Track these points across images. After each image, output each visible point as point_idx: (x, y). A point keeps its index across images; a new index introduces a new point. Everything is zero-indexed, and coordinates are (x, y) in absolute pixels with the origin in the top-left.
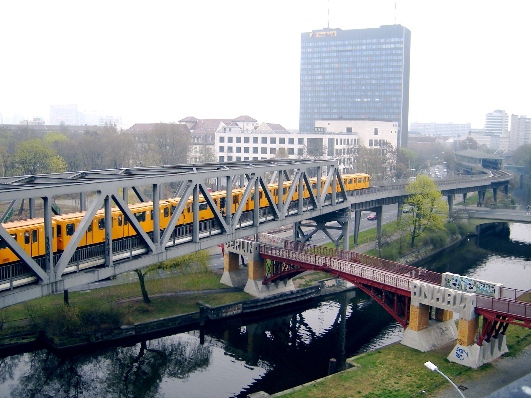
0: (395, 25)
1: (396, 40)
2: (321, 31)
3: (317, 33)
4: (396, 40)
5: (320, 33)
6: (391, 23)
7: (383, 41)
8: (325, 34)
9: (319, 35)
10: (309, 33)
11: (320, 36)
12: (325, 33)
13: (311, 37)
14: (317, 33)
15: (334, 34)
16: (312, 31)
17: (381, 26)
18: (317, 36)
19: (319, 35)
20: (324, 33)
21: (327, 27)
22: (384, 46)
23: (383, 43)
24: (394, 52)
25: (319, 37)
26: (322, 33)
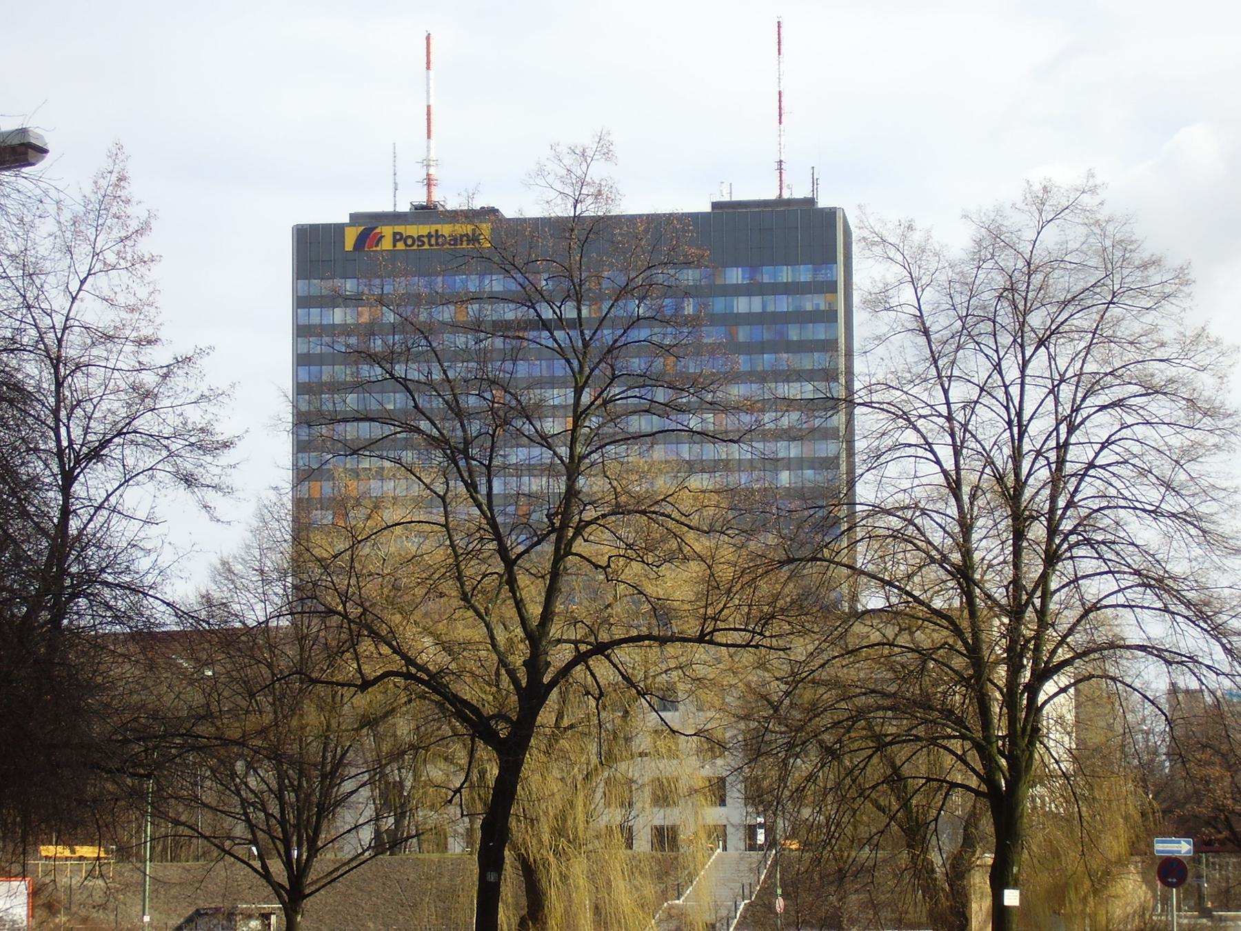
0: (780, 202)
1: (804, 274)
2: (395, 218)
3: (387, 231)
4: (804, 274)
5: (398, 229)
6: (762, 189)
7: (735, 276)
8: (429, 236)
9: (397, 237)
10: (339, 229)
11: (400, 246)
12: (433, 228)
13: (349, 245)
14: (387, 231)
15: (474, 239)
16: (347, 220)
17: (715, 205)
18: (387, 244)
19: (397, 237)
20: (424, 230)
21: (422, 199)
22: (742, 305)
23: (737, 291)
24: (794, 334)
25: (393, 253)
26: (413, 230)
